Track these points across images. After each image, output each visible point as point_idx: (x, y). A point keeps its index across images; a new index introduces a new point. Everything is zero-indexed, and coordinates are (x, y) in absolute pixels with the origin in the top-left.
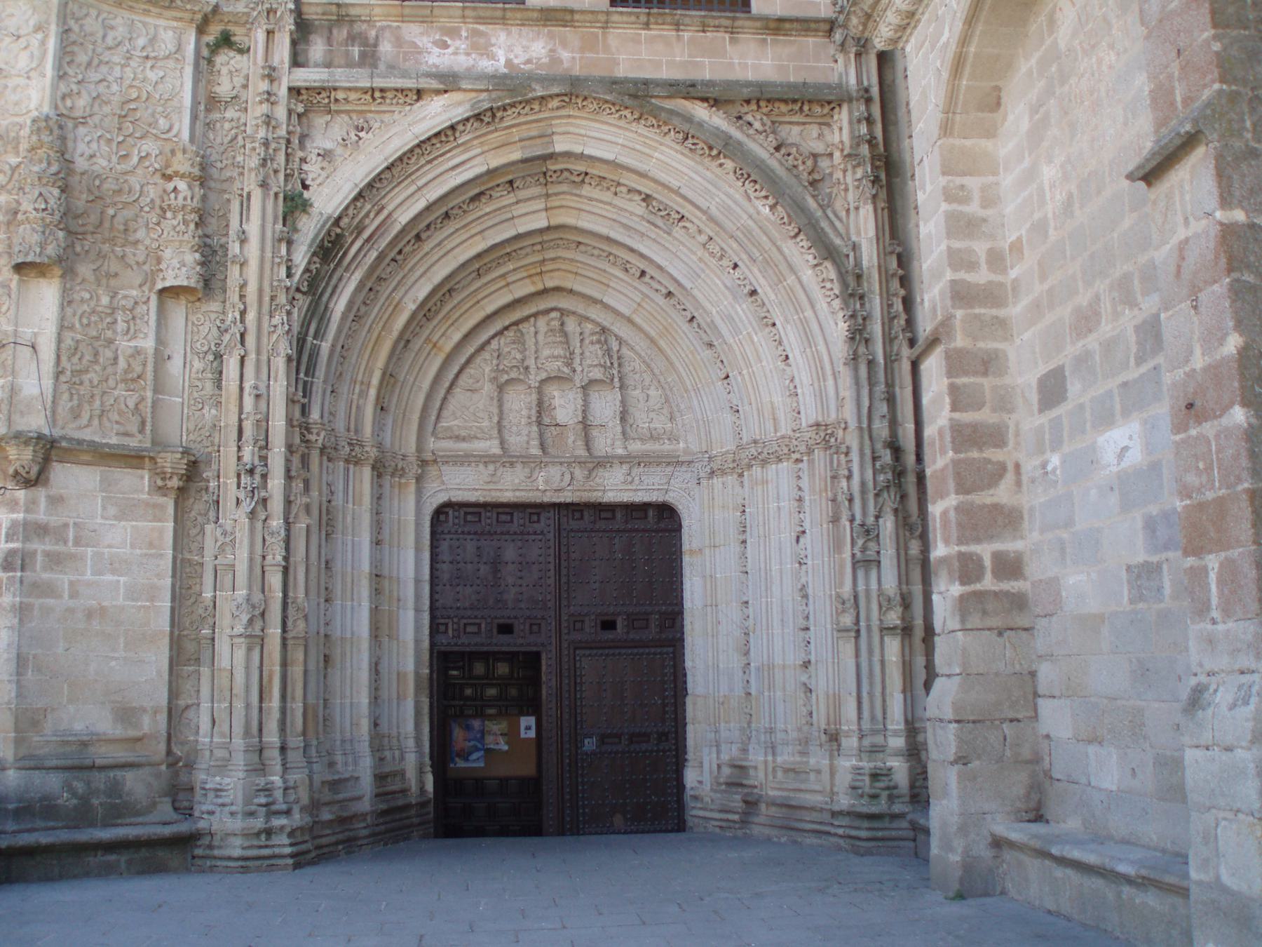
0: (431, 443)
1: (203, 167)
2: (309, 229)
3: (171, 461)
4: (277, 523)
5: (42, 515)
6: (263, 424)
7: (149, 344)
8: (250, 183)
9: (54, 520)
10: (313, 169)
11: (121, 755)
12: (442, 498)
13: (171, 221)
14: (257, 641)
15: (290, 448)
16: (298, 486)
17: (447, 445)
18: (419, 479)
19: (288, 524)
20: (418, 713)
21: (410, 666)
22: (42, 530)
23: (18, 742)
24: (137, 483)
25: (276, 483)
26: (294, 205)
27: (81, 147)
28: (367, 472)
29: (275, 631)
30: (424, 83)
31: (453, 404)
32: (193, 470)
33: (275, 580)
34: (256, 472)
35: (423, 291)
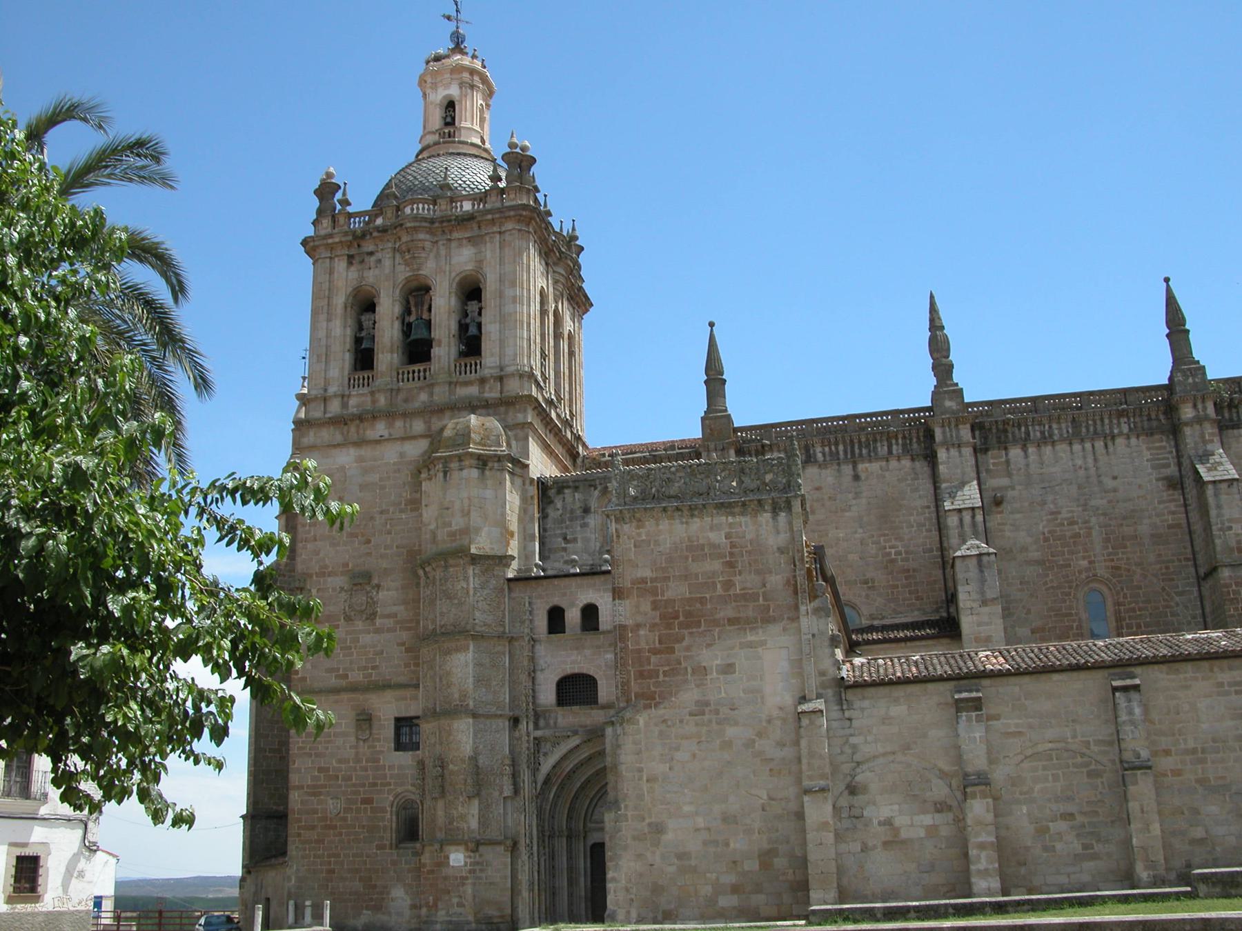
0: (589, 825)
1: (513, 761)
2: (541, 777)
3: (509, 842)
4: (536, 859)
5: (478, 859)
6: (531, 834)
7: (502, 811)
8: (525, 766)
9: (481, 860)
10: (542, 759)
11: (500, 920)
12: (593, 842)
13: (505, 778)
14: (531, 890)
15: (538, 838)
16: (541, 848)
17: (593, 825)
18: (585, 838)
19: (539, 860)
20: (586, 908)
21: (583, 893)
22: (478, 863)
23: (475, 916)
24: (501, 849)
25: (535, 848)
26: (535, 772)
27: (481, 761)
28: (565, 839)
29: (536, 887)
30: (569, 733)
31: (596, 811)
32: (515, 844)
33: (536, 874)
34: (530, 846)
35: (578, 785)
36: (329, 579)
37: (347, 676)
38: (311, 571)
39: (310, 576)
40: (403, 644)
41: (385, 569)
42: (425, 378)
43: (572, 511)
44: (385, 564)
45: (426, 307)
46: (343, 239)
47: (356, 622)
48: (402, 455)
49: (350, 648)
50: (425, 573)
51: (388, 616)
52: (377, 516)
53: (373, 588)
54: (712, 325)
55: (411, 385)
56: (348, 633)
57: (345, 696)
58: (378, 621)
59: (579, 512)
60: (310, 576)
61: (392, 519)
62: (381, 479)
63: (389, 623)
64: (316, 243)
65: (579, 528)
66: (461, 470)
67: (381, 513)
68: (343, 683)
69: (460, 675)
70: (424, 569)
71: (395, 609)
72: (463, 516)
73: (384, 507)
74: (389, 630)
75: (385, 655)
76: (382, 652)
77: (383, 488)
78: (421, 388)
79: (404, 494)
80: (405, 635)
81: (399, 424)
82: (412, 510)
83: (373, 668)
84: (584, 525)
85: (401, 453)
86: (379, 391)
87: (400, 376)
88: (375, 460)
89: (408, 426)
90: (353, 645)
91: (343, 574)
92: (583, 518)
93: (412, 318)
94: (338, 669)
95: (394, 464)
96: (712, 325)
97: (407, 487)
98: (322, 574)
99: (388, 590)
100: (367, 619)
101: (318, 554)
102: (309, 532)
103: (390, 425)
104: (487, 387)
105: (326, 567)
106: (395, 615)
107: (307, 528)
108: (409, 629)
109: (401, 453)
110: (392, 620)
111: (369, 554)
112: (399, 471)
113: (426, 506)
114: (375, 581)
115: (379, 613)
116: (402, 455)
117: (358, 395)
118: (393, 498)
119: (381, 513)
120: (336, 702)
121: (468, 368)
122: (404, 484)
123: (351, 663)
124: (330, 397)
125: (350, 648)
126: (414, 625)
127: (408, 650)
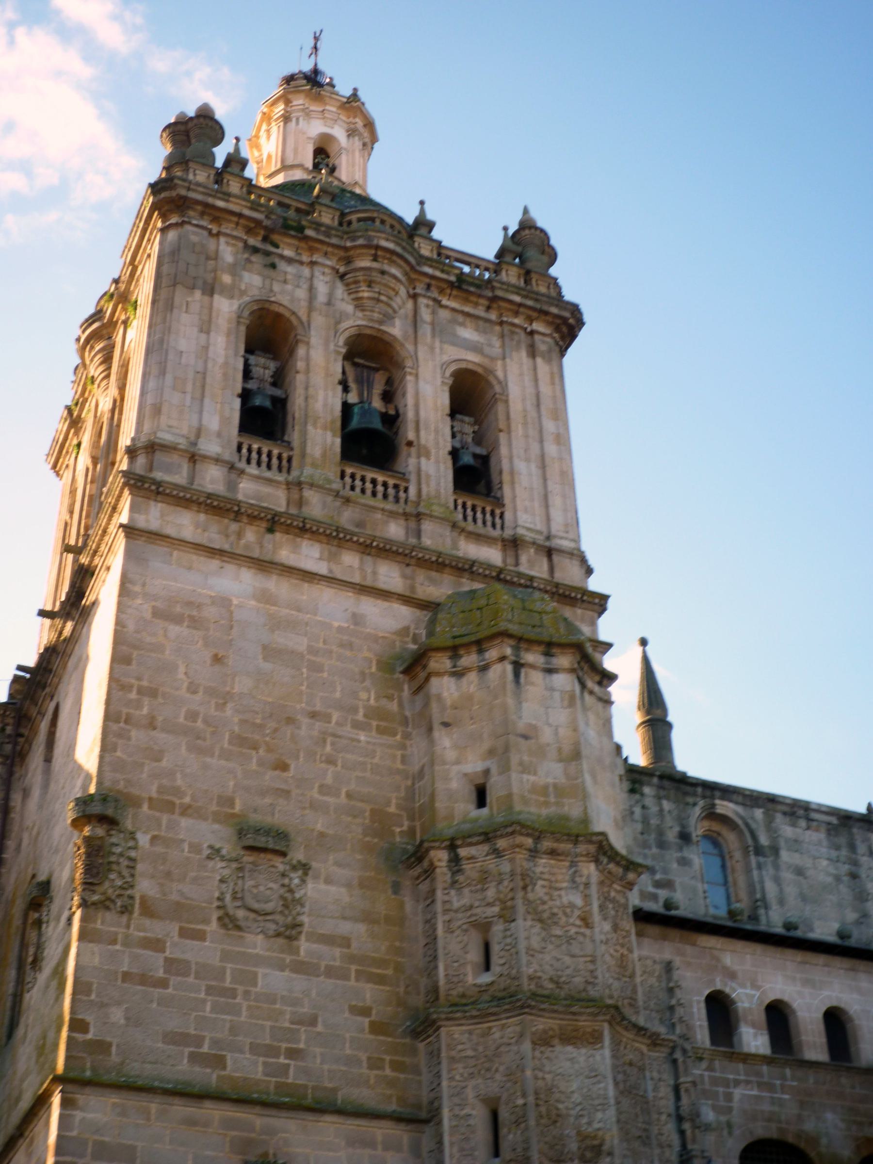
36: (185, 822)
37: (219, 1062)
38: (135, 791)
39: (136, 802)
40: (365, 1012)
41: (322, 835)
42: (397, 500)
43: (661, 833)
44: (320, 824)
45: (378, 388)
46: (247, 212)
47: (249, 937)
48: (357, 619)
49: (233, 994)
50: (455, 860)
51: (329, 940)
52: (305, 721)
53: (294, 868)
54: (644, 642)
55: (368, 500)
56: (226, 956)
57: (214, 1112)
58: (304, 946)
59: (671, 835)
60: (136, 802)
61: (334, 735)
62: (312, 650)
63: (333, 955)
64: (192, 195)
65: (675, 865)
66: (550, 671)
67: (313, 715)
68: (211, 1077)
69: (577, 1098)
70: (452, 847)
71: (345, 928)
72: (561, 760)
73: (318, 707)
74: (330, 972)
75: (320, 1028)
76: (312, 1021)
77: (316, 668)
78: (392, 514)
79: (363, 695)
80: (369, 993)
81: (350, 559)
82: (381, 731)
83: (293, 1054)
84: (684, 862)
85: (354, 615)
86: (312, 485)
87: (348, 480)
88: (299, 610)
89: (369, 570)
90: (240, 989)
91: (217, 818)
92: (680, 849)
93: (353, 398)
94: (199, 1041)
95: (340, 629)
96: (644, 642)
97: (368, 683)
98: (169, 807)
99: (328, 881)
100: (278, 935)
101: (159, 760)
102: (139, 705)
103: (332, 558)
104: (523, 559)
105: (177, 792)
106: (345, 942)
107: (133, 695)
108: (380, 980)
109: (354, 615)
110: (337, 952)
111: (286, 793)
112: (350, 646)
113: (446, 725)
114: (298, 855)
115: (306, 928)
116: (357, 619)
117: (258, 478)
118: (338, 695)
119: (313, 715)
120: (191, 1122)
121: (479, 515)
122: (363, 674)
123: (231, 1029)
124: (205, 457)
125: (233, 994)
126: (390, 972)
127: (377, 1028)
